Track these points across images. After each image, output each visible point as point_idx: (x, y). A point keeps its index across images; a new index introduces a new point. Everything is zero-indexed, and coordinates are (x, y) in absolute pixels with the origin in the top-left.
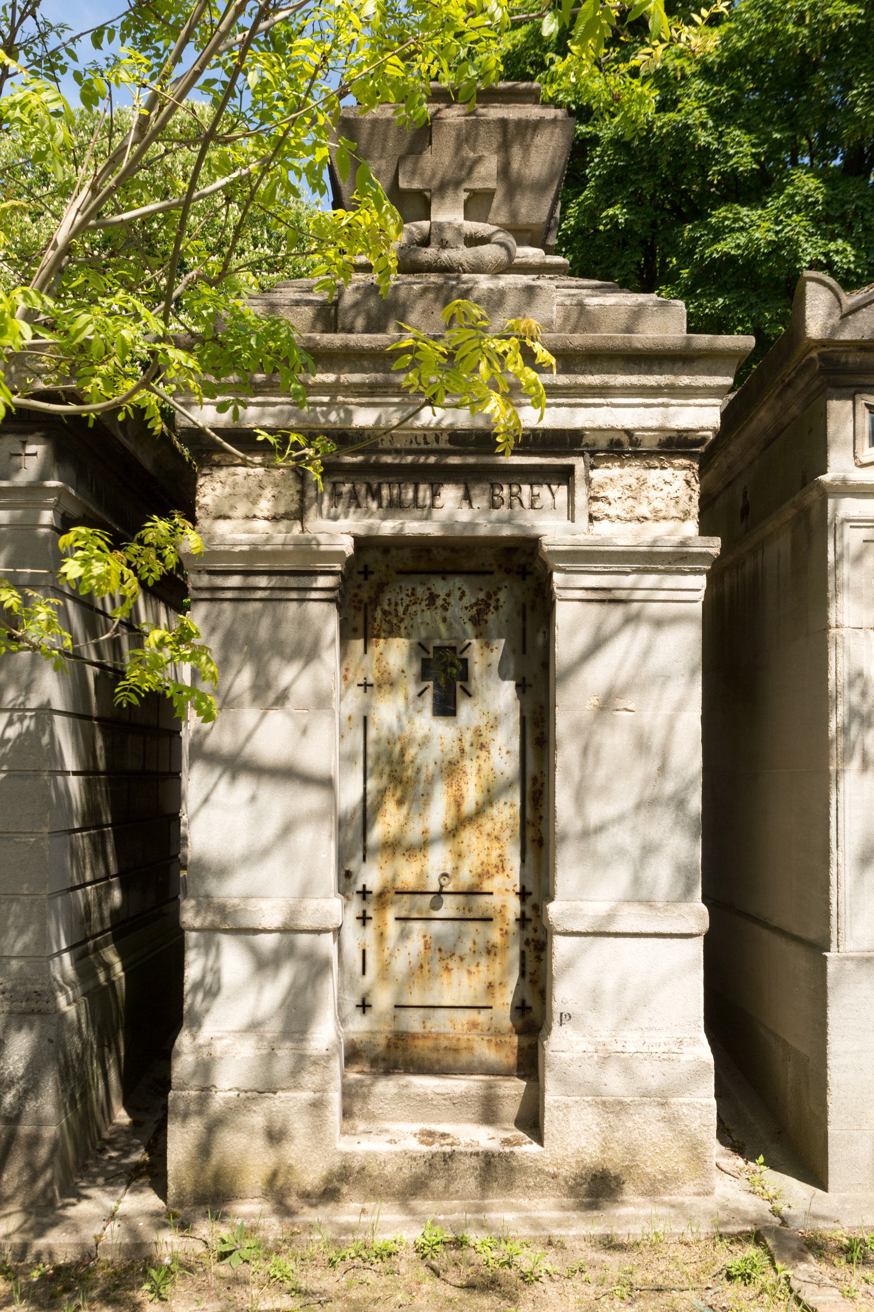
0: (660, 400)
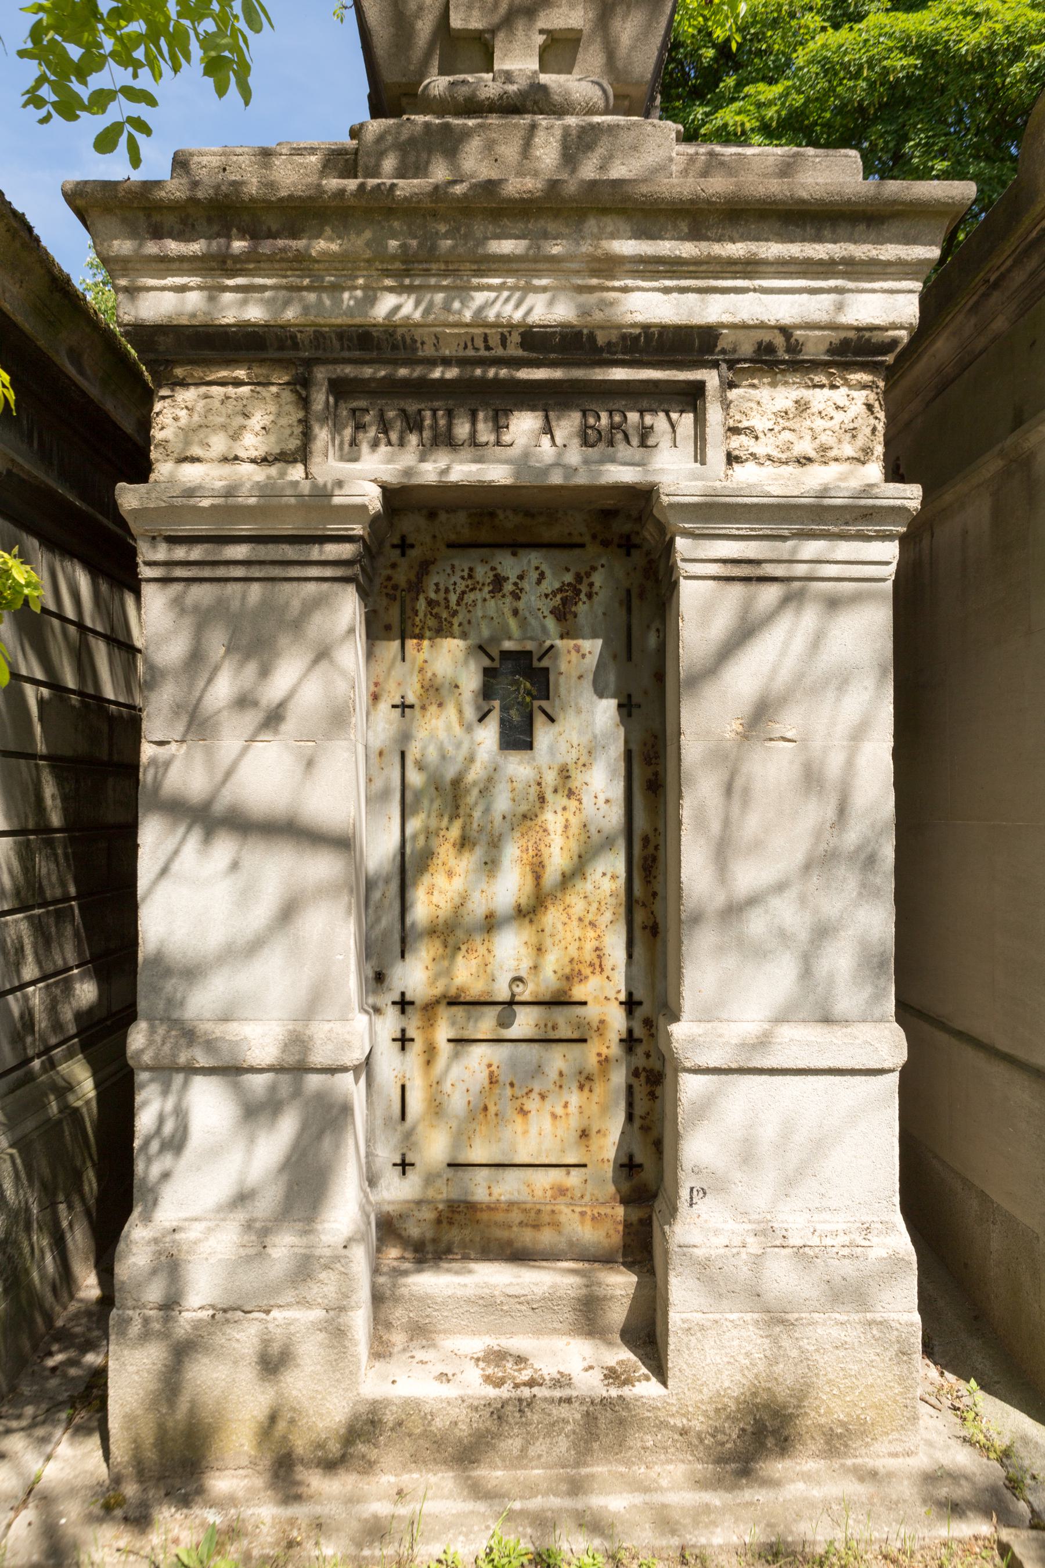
0: (832, 283)
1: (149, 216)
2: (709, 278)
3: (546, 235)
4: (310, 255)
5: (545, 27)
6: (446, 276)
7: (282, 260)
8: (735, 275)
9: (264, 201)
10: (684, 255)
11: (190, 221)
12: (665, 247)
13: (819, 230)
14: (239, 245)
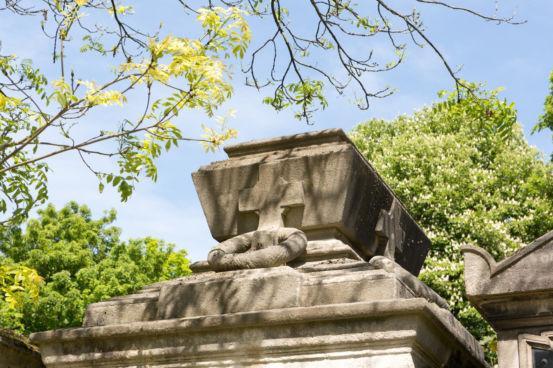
0: (364, 352)
1: (63, 345)
2: (304, 354)
3: (226, 341)
4: (126, 358)
5: (283, 205)
6: (184, 362)
7: (115, 360)
8: (316, 352)
9: (106, 336)
10: (289, 345)
11: (79, 346)
12: (280, 342)
13: (353, 327)
14: (98, 355)
